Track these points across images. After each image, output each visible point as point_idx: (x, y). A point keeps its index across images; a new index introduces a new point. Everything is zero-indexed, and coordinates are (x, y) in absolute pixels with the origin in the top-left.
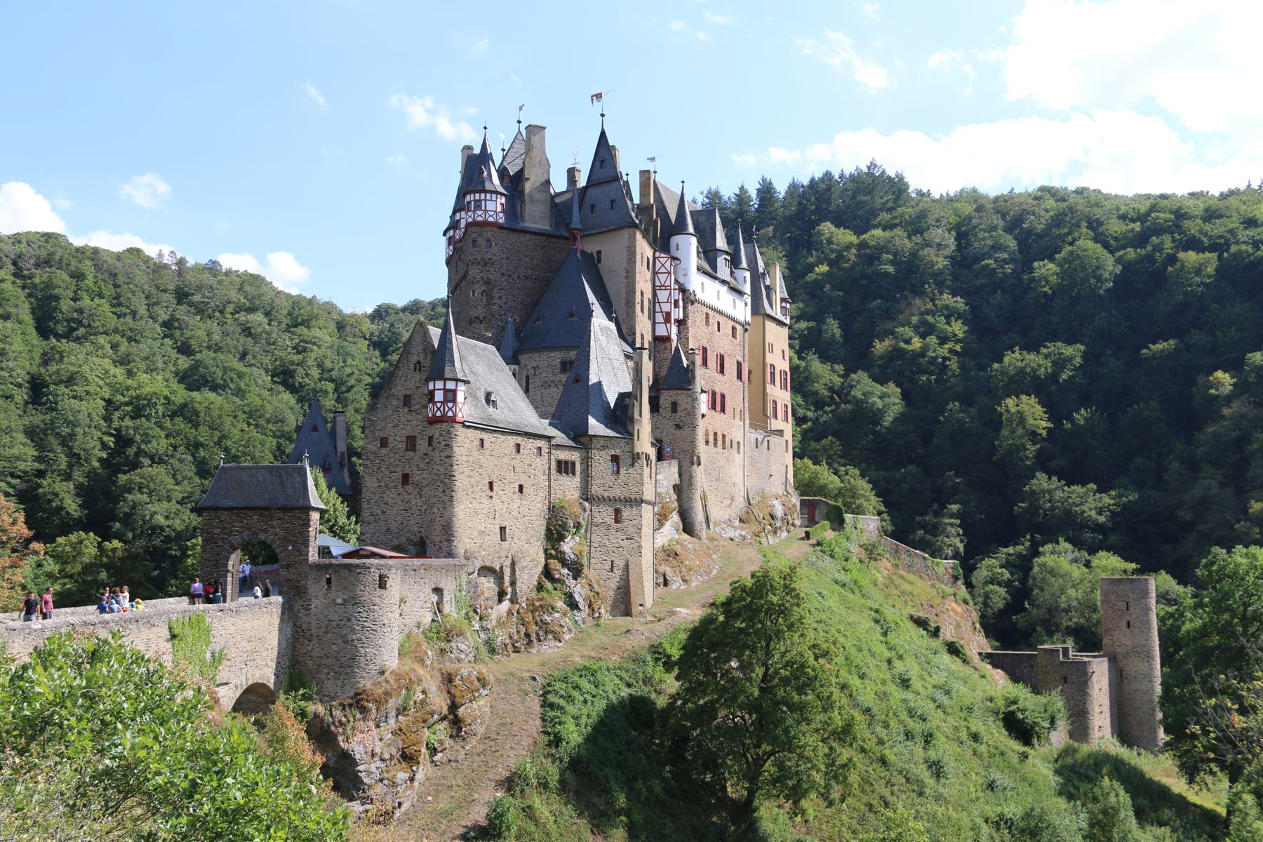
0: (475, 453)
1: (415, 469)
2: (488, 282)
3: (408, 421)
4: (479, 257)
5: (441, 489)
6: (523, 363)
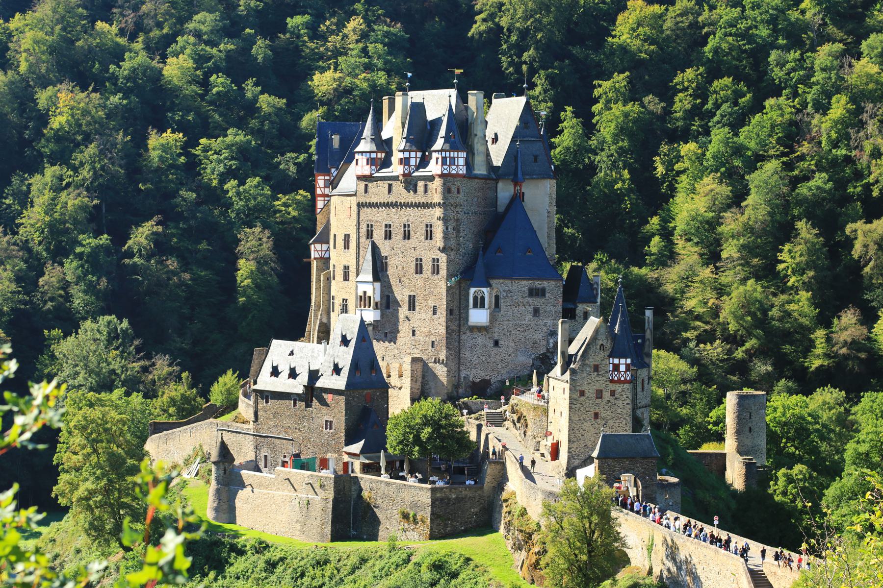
1: (602, 409)
2: (457, 220)
4: (452, 201)
5: (624, 423)
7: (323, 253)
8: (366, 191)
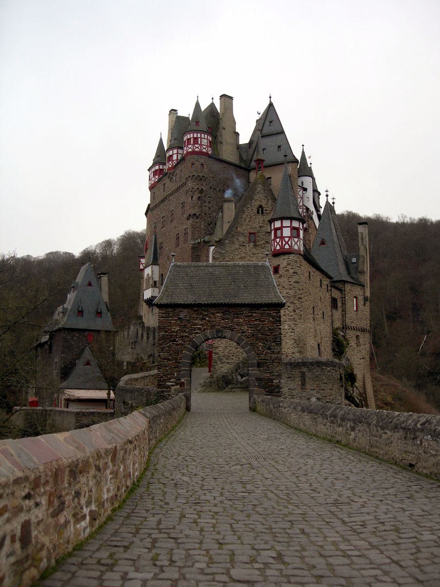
0: (308, 282)
2: (201, 191)
3: (254, 254)
4: (196, 175)
5: (291, 309)
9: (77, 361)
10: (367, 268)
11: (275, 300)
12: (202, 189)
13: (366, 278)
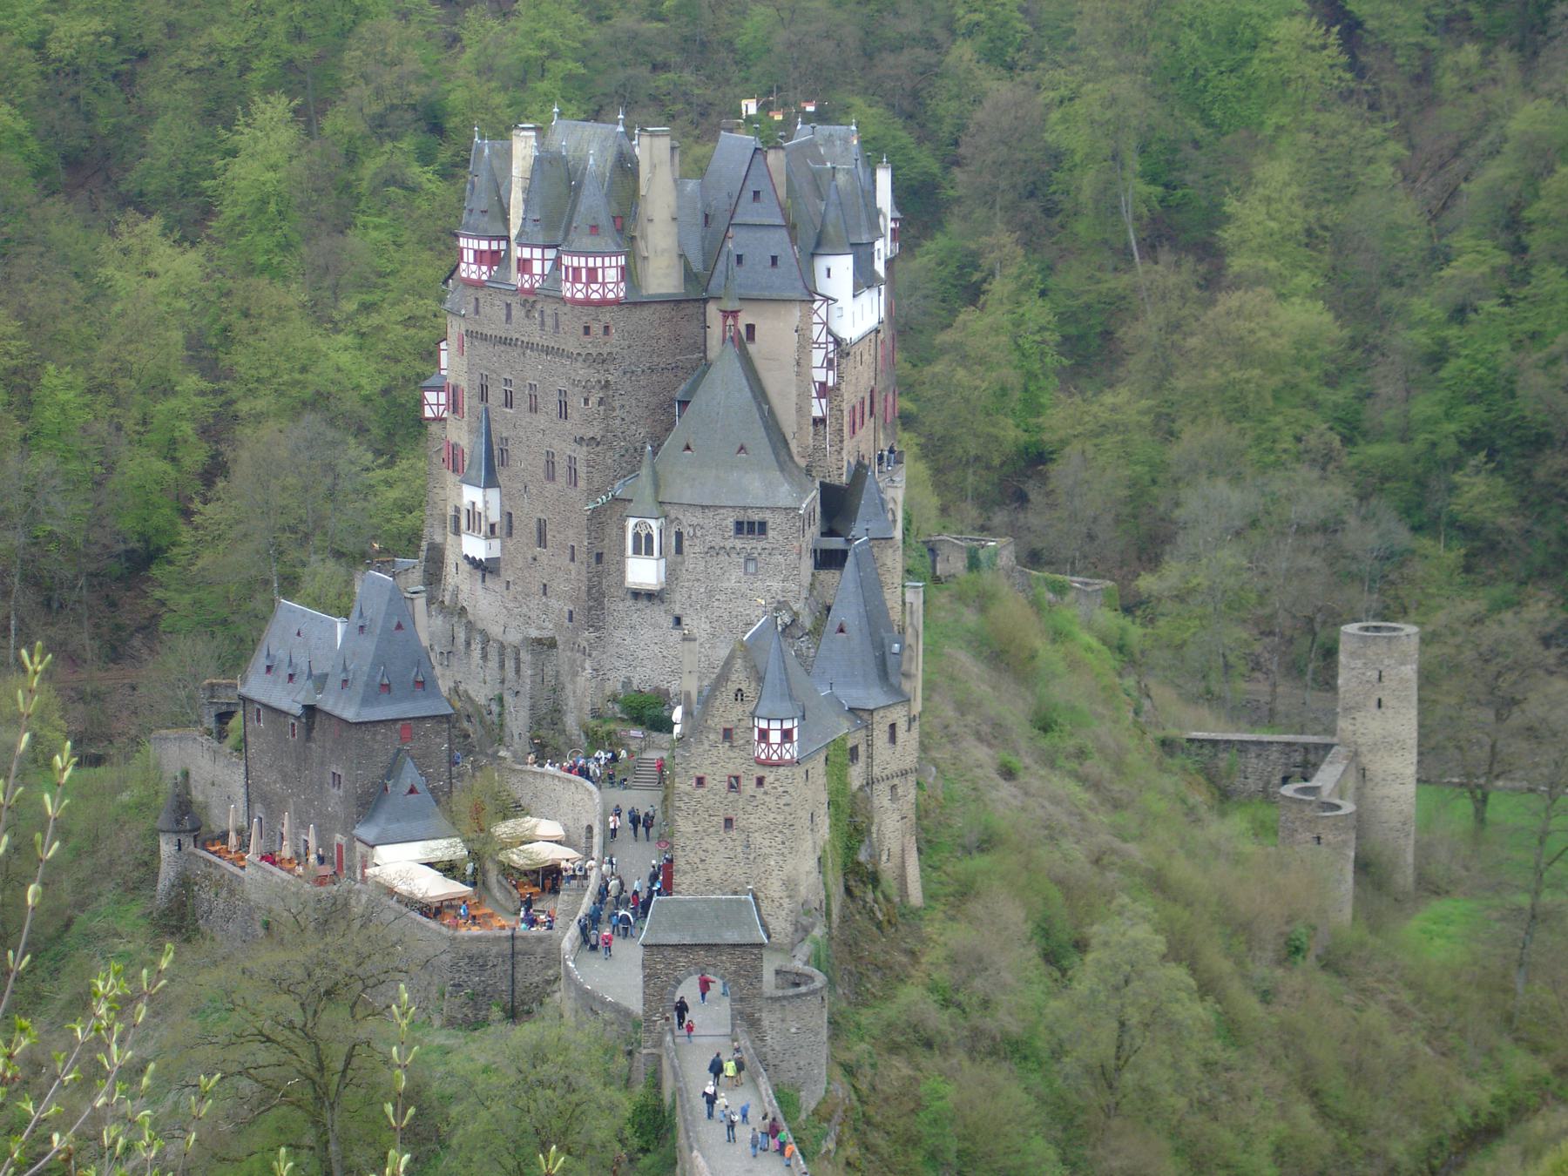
6: (673, 516)
7: (441, 408)
8: (477, 312)
9: (390, 784)
10: (918, 667)
11: (758, 941)
12: (607, 381)
13: (915, 687)
